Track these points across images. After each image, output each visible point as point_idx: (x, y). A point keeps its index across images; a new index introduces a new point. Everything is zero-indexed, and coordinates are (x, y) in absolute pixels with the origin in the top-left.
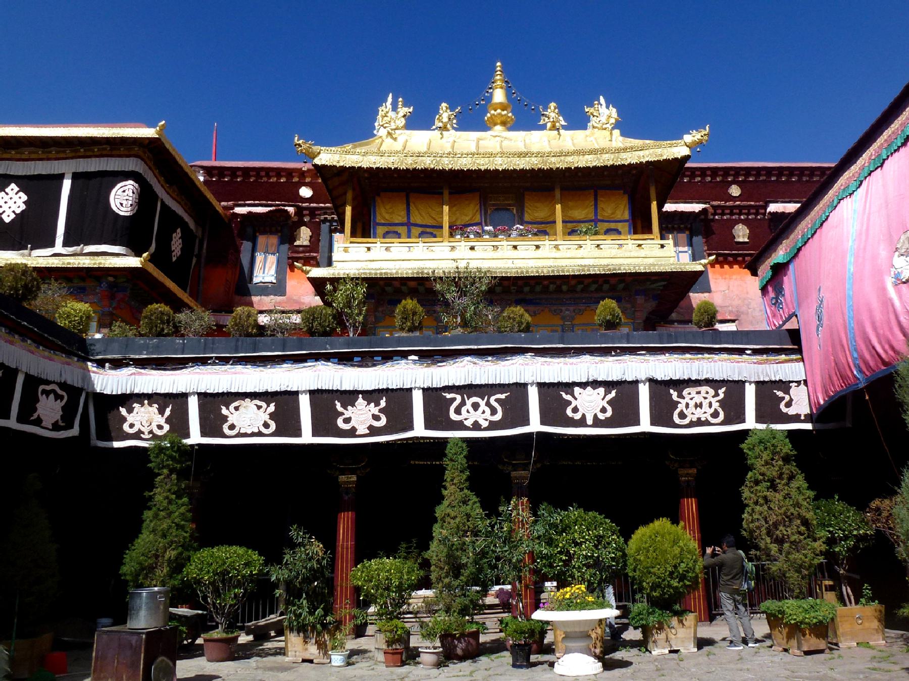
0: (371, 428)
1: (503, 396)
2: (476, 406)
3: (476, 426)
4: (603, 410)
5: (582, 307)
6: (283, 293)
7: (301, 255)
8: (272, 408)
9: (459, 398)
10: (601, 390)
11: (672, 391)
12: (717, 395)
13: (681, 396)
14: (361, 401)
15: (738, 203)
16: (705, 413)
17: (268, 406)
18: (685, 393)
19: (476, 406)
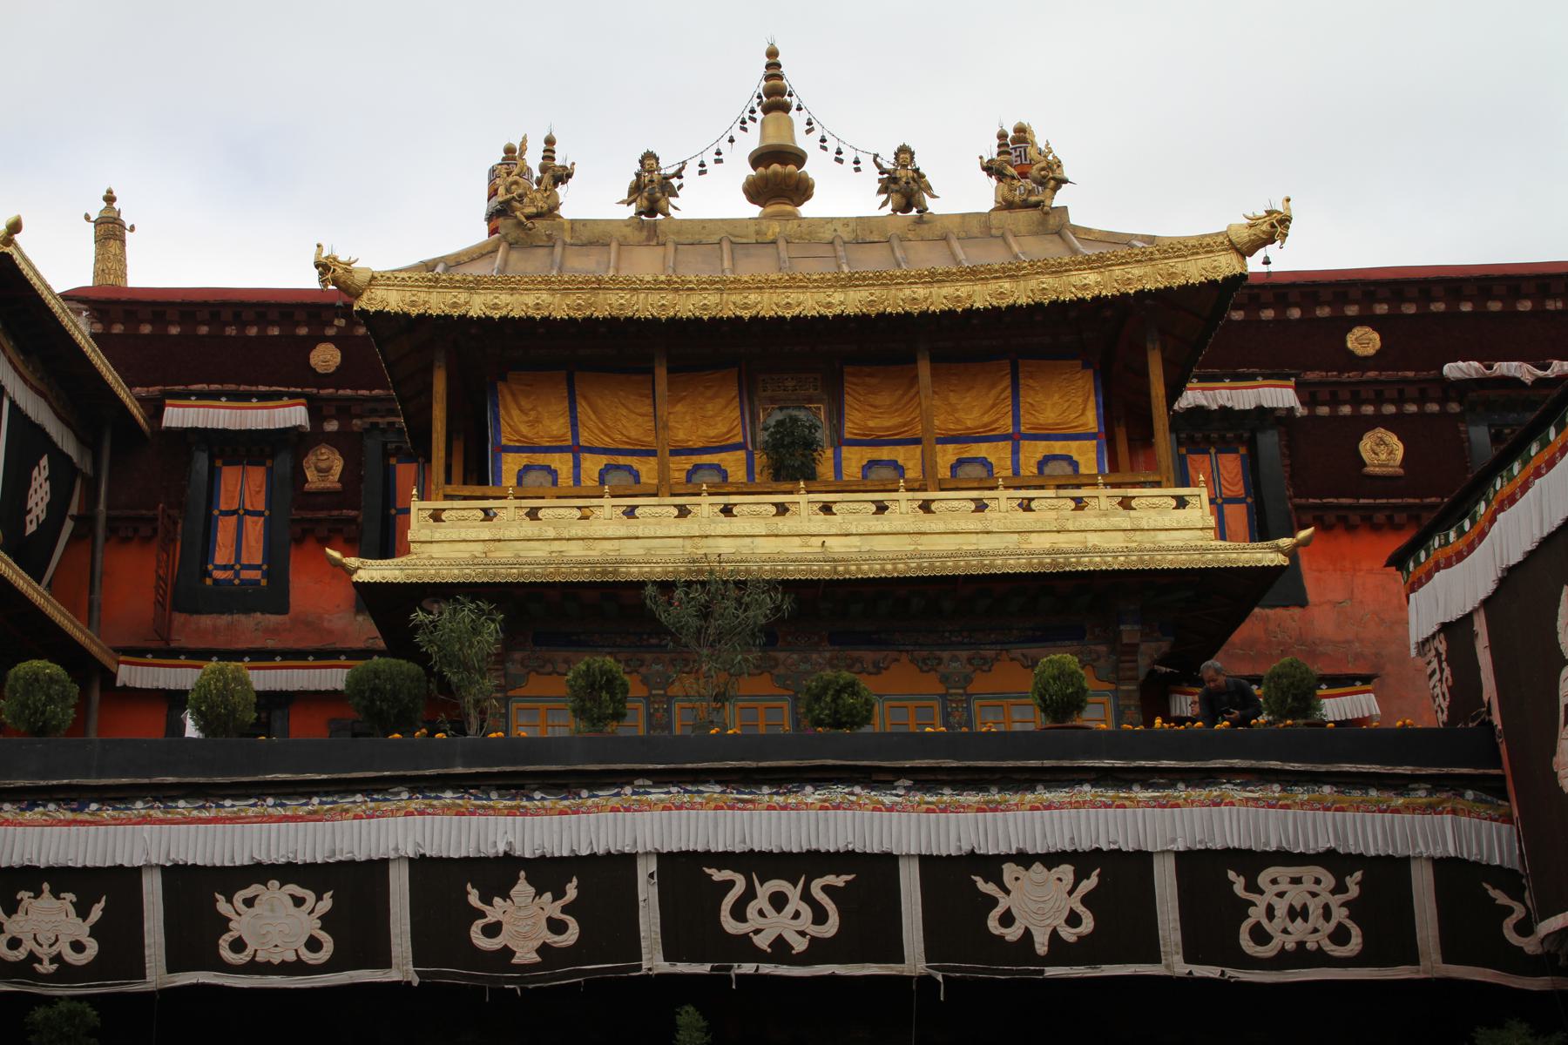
0: (544, 949)
1: (839, 881)
2: (778, 901)
4: (1073, 920)
5: (990, 653)
6: (282, 607)
7: (322, 515)
8: (326, 904)
10: (1066, 871)
11: (1231, 875)
13: (1252, 886)
14: (522, 889)
15: (1372, 374)
16: (1312, 933)
17: (319, 898)
18: (1263, 879)
19: (778, 901)
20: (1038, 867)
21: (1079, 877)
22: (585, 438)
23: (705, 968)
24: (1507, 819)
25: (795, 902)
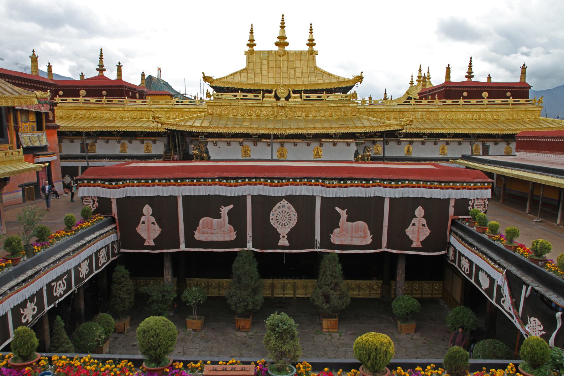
1: (65, 277)
3: (61, 296)
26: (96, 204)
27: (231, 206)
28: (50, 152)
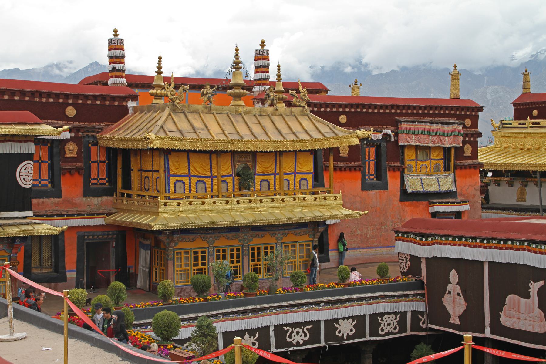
1: (309, 327)
2: (298, 333)
3: (298, 344)
4: (351, 331)
9: (290, 329)
10: (351, 320)
12: (396, 319)
13: (382, 320)
14: (247, 336)
16: (390, 329)
19: (298, 333)
20: (346, 320)
21: (353, 321)
22: (192, 173)
23: (283, 350)
24: (424, 301)
25: (301, 333)
26: (409, 263)
27: (542, 283)
28: (460, 199)
